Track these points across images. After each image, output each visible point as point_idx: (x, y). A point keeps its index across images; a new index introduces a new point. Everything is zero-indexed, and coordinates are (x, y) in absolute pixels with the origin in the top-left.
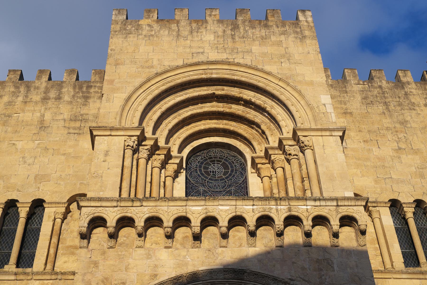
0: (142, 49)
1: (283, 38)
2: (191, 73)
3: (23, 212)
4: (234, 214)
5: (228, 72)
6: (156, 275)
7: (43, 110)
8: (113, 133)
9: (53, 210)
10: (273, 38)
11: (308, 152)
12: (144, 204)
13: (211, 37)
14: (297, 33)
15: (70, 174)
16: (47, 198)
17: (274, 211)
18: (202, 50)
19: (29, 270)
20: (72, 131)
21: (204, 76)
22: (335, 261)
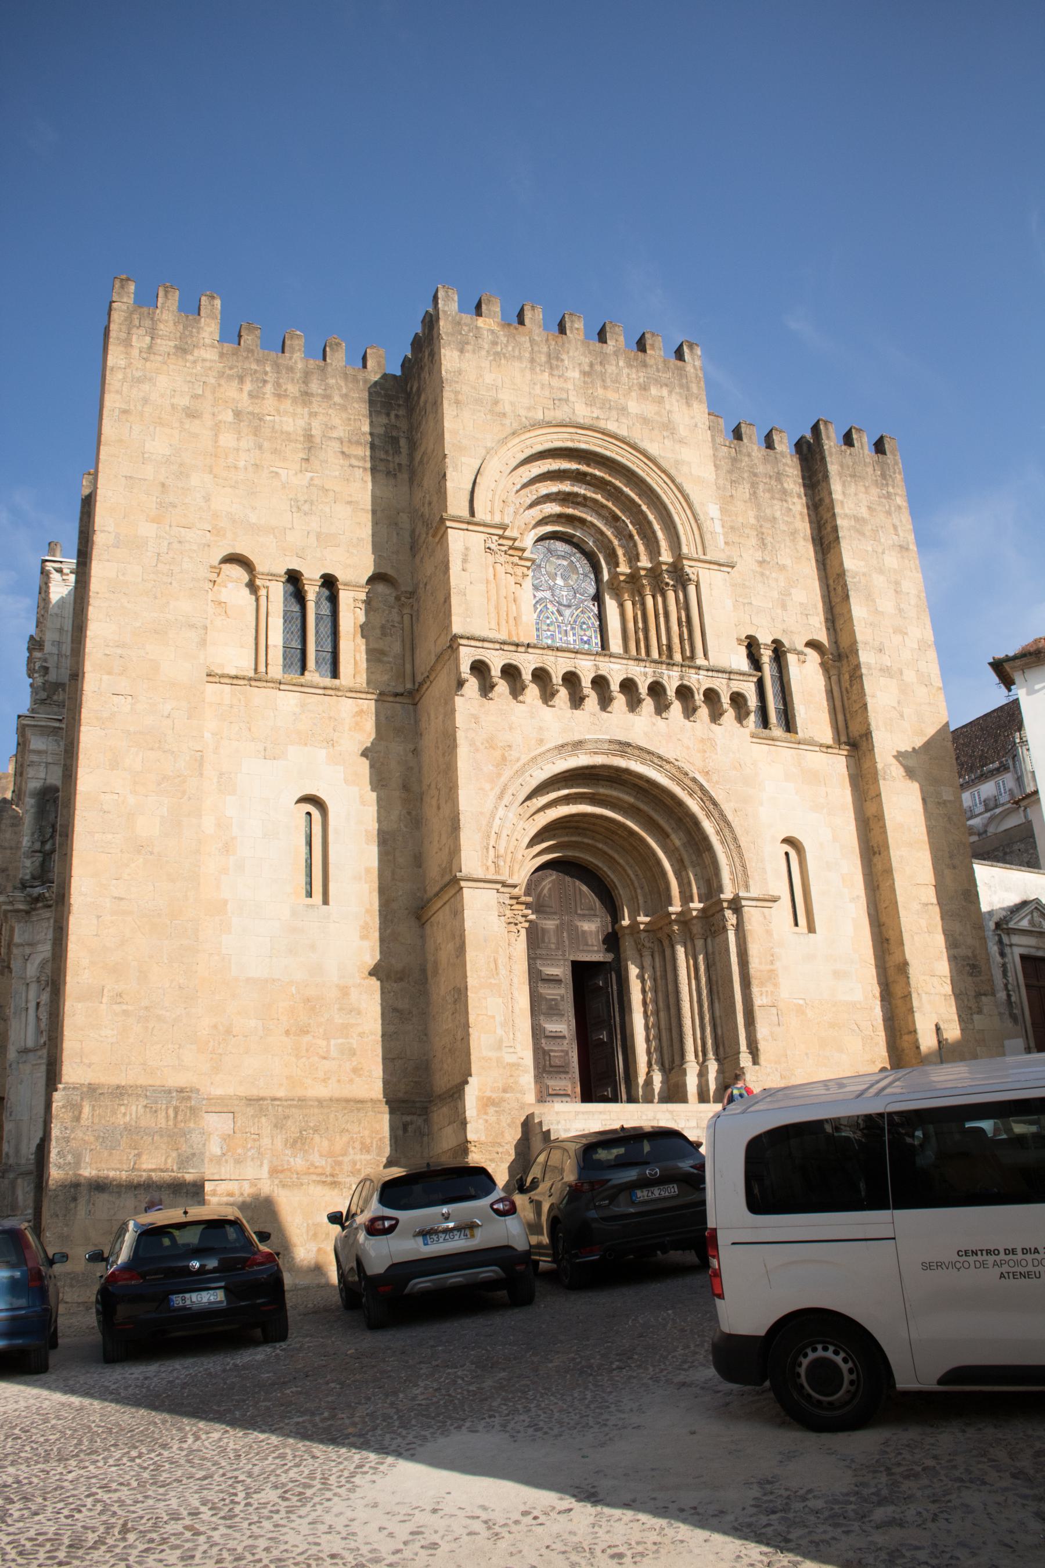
0: (489, 378)
1: (665, 392)
2: (555, 436)
3: (312, 592)
4: (625, 676)
5: (600, 442)
6: (541, 741)
7: (306, 416)
8: (471, 527)
9: (351, 594)
10: (654, 391)
11: (692, 589)
12: (530, 650)
13: (575, 374)
14: (681, 386)
15: (363, 539)
16: (340, 575)
17: (665, 677)
18: (564, 396)
19: (336, 682)
20: (355, 462)
21: (570, 444)
22: (718, 742)
